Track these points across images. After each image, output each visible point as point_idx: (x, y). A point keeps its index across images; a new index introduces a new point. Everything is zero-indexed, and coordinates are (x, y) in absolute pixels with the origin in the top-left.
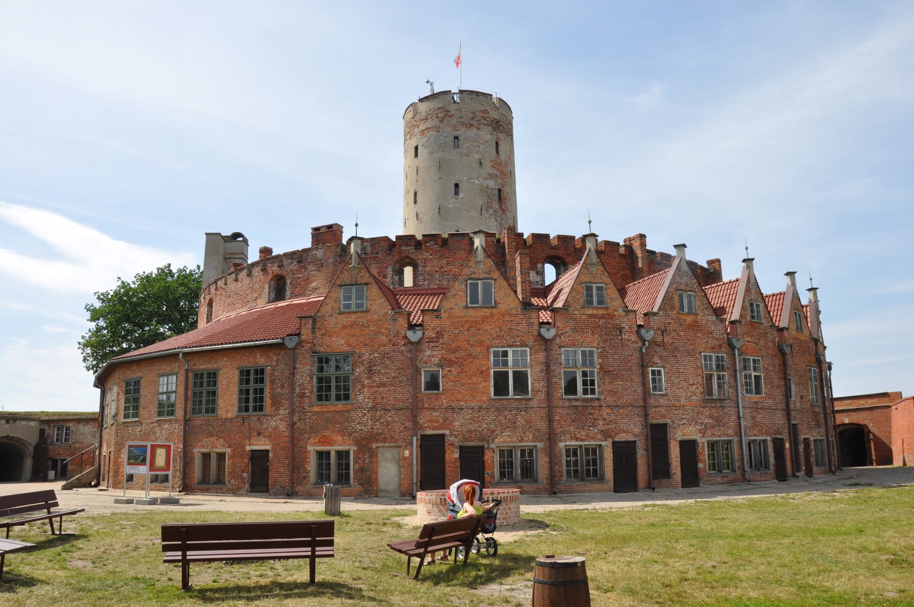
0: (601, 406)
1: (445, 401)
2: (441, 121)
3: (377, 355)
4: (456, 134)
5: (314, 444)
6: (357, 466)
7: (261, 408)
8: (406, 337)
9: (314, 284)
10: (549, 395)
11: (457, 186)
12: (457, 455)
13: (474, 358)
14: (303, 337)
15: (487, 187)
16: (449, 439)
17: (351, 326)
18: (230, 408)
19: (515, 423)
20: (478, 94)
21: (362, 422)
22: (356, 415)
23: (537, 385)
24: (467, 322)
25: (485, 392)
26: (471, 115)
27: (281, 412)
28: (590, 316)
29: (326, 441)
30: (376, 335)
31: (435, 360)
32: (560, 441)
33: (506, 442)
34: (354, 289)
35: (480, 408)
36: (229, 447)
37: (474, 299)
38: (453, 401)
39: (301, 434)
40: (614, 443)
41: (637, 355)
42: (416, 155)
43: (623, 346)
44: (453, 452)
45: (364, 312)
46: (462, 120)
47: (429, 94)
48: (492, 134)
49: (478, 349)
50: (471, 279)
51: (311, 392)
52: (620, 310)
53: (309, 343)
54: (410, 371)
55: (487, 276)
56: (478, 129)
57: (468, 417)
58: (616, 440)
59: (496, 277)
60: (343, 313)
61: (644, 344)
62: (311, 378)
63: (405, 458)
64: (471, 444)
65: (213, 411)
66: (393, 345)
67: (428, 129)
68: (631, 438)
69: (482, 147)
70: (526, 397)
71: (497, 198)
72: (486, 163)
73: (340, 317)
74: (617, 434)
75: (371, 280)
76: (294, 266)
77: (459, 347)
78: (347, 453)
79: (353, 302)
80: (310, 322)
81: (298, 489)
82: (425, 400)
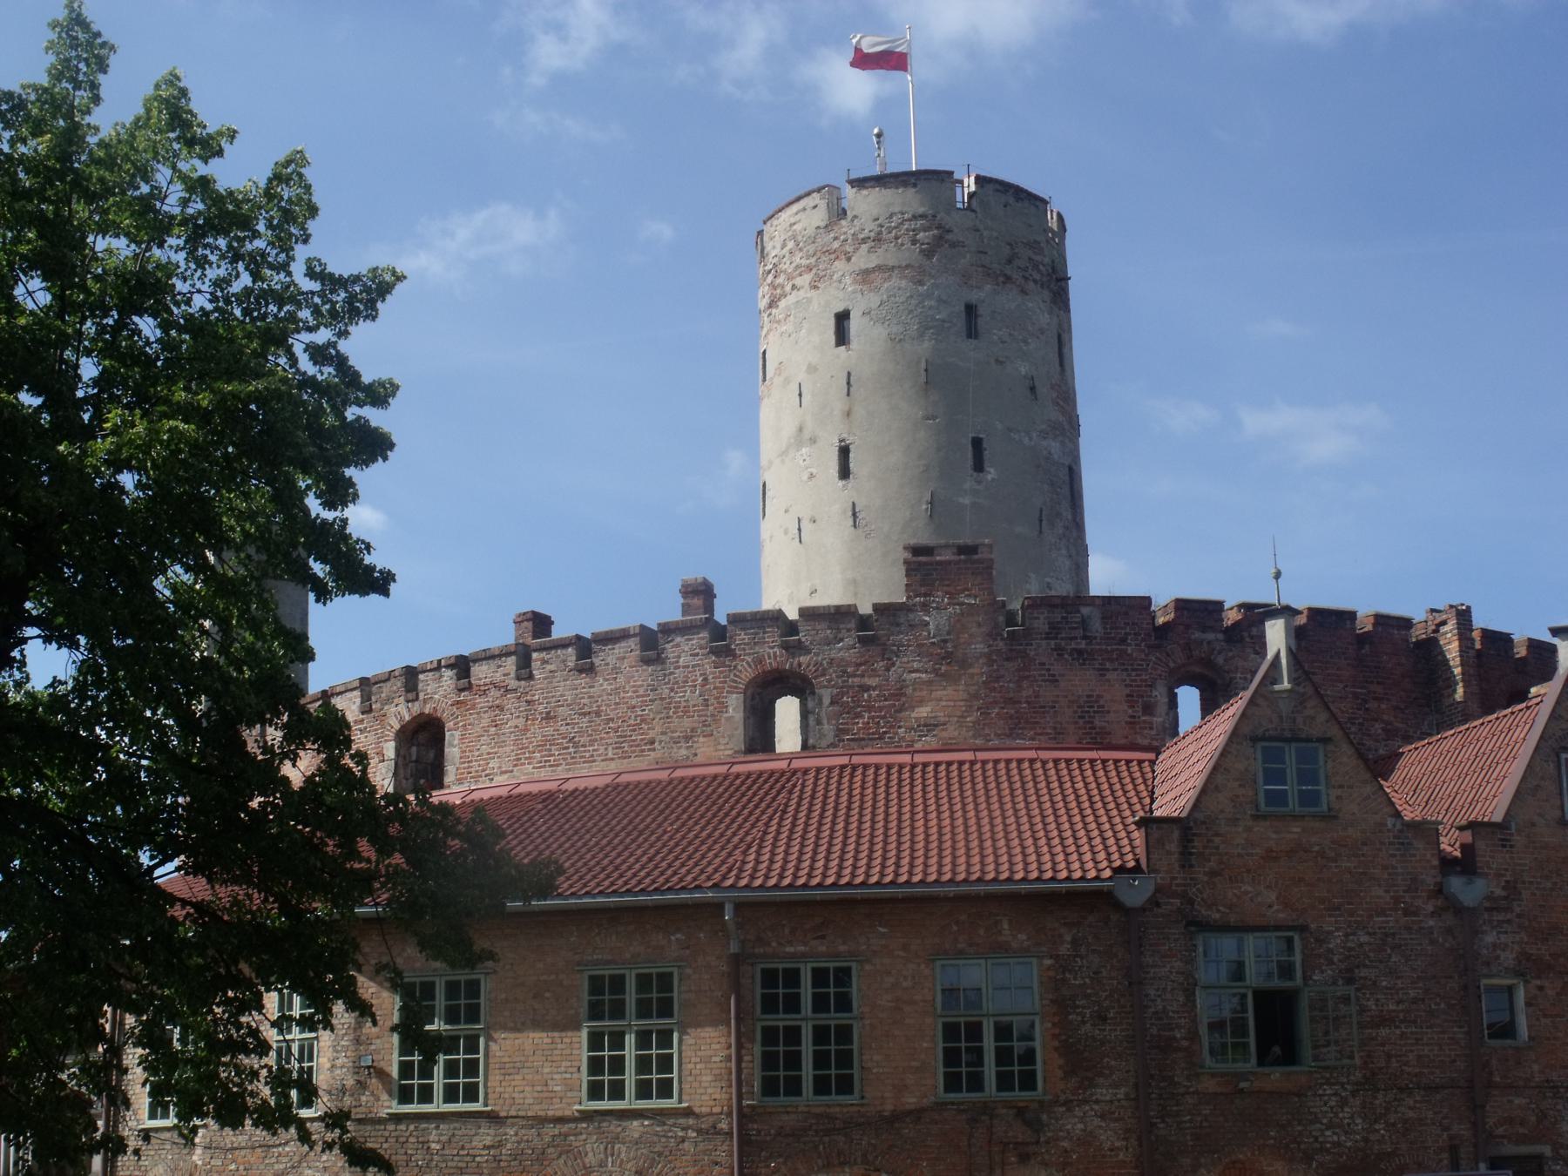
1: (1536, 1067)
3: (1364, 939)
4: (974, 296)
7: (1028, 1082)
8: (1439, 891)
9: (923, 712)
11: (977, 444)
26: (1007, 251)
27: (1103, 1093)
31: (1508, 958)
42: (842, 338)
45: (1323, 817)
48: (1050, 313)
56: (1024, 292)
60: (1265, 817)
65: (845, 1086)
66: (1406, 913)
71: (1066, 490)
75: (1334, 731)
76: (846, 648)
79: (1291, 787)
80: (1176, 835)
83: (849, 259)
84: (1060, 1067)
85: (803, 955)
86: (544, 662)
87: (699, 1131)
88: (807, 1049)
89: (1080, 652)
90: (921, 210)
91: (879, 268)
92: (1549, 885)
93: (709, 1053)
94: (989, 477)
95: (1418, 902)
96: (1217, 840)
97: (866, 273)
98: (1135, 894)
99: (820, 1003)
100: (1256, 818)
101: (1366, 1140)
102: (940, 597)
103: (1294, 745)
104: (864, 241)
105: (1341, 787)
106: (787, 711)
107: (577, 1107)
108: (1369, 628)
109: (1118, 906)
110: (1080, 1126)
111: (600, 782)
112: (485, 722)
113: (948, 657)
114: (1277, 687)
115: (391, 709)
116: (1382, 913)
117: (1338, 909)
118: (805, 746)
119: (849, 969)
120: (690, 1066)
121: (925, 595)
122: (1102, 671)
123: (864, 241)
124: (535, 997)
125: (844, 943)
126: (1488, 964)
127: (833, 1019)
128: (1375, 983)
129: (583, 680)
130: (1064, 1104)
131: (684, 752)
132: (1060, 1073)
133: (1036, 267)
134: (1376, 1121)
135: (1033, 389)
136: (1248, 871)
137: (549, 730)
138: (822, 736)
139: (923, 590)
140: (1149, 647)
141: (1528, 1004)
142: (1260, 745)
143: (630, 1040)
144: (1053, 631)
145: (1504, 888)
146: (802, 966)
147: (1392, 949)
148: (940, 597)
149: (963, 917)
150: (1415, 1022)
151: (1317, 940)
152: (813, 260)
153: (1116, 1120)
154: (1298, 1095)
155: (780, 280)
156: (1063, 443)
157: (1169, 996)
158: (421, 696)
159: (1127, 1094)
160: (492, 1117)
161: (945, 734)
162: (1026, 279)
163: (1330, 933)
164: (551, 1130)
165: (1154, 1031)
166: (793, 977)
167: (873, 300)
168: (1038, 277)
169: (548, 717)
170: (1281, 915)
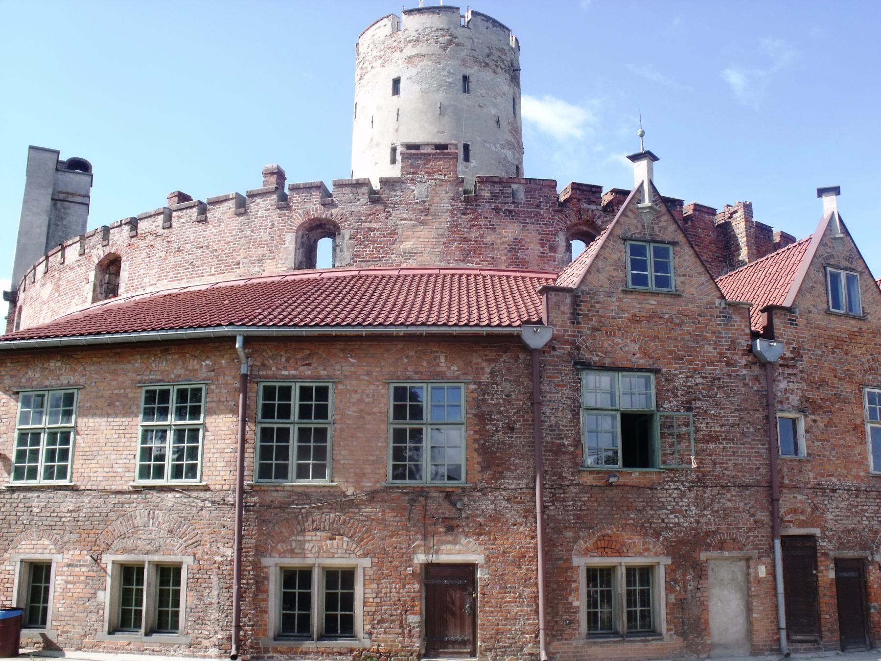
1: (811, 475)
4: (467, 72)
5: (586, 552)
6: (672, 598)
8: (750, 350)
12: (832, 575)
15: (505, 159)
16: (823, 544)
17: (649, 318)
18: (368, 469)
20: (495, 22)
21: (680, 509)
22: (669, 494)
24: (830, 337)
25: (862, 462)
26: (487, 51)
27: (509, 483)
29: (607, 546)
30: (696, 341)
31: (794, 399)
36: (365, 555)
38: (822, 475)
42: (396, 90)
44: (827, 569)
45: (671, 295)
46: (475, 54)
48: (510, 86)
53: (566, 342)
54: (759, 415)
56: (495, 72)
59: (860, 269)
63: (759, 581)
69: (499, 100)
72: (503, 123)
73: (628, 299)
75: (680, 238)
76: (362, 205)
79: (651, 273)
80: (568, 300)
82: (785, 470)
83: (401, 51)
84: (479, 463)
85: (294, 377)
86: (179, 217)
87: (213, 502)
88: (294, 443)
89: (510, 212)
90: (441, 26)
91: (417, 55)
92: (820, 352)
93: (224, 446)
94: (472, 165)
95: (736, 358)
96: (597, 306)
97: (410, 57)
98: (536, 339)
99: (305, 412)
100: (625, 292)
101: (698, 522)
102: (422, 175)
103: (652, 245)
104: (410, 42)
105: (684, 275)
106: (324, 246)
107: (132, 484)
108: (691, 212)
110: (492, 507)
111: (203, 288)
112: (144, 254)
113: (427, 211)
114: (640, 205)
115: (94, 252)
116: (712, 363)
117: (682, 359)
118: (334, 266)
119: (327, 388)
120: (210, 455)
121: (413, 173)
122: (525, 224)
123: (410, 42)
124: (109, 405)
125: (325, 369)
126: (781, 403)
127: (313, 423)
128: (706, 412)
129: (201, 227)
130: (481, 490)
131: (257, 269)
132: (478, 468)
133: (502, 61)
134: (705, 509)
135: (498, 122)
136: (619, 329)
137: (179, 259)
138: (343, 259)
140: (555, 211)
141: (807, 431)
142: (629, 243)
143: (170, 435)
144: (494, 196)
145: (792, 352)
146: (293, 385)
147: (718, 388)
148: (422, 175)
149: (412, 353)
150: (732, 440)
151: (666, 380)
152: (382, 53)
153: (519, 503)
154: (652, 489)
155: (366, 65)
156: (514, 153)
157: (560, 414)
158: (111, 243)
159: (527, 484)
160: (73, 489)
161: (421, 259)
163: (675, 375)
164: (113, 499)
165: (549, 439)
166: (286, 393)
167: (413, 71)
168: (501, 64)
169: (179, 250)
170: (642, 361)
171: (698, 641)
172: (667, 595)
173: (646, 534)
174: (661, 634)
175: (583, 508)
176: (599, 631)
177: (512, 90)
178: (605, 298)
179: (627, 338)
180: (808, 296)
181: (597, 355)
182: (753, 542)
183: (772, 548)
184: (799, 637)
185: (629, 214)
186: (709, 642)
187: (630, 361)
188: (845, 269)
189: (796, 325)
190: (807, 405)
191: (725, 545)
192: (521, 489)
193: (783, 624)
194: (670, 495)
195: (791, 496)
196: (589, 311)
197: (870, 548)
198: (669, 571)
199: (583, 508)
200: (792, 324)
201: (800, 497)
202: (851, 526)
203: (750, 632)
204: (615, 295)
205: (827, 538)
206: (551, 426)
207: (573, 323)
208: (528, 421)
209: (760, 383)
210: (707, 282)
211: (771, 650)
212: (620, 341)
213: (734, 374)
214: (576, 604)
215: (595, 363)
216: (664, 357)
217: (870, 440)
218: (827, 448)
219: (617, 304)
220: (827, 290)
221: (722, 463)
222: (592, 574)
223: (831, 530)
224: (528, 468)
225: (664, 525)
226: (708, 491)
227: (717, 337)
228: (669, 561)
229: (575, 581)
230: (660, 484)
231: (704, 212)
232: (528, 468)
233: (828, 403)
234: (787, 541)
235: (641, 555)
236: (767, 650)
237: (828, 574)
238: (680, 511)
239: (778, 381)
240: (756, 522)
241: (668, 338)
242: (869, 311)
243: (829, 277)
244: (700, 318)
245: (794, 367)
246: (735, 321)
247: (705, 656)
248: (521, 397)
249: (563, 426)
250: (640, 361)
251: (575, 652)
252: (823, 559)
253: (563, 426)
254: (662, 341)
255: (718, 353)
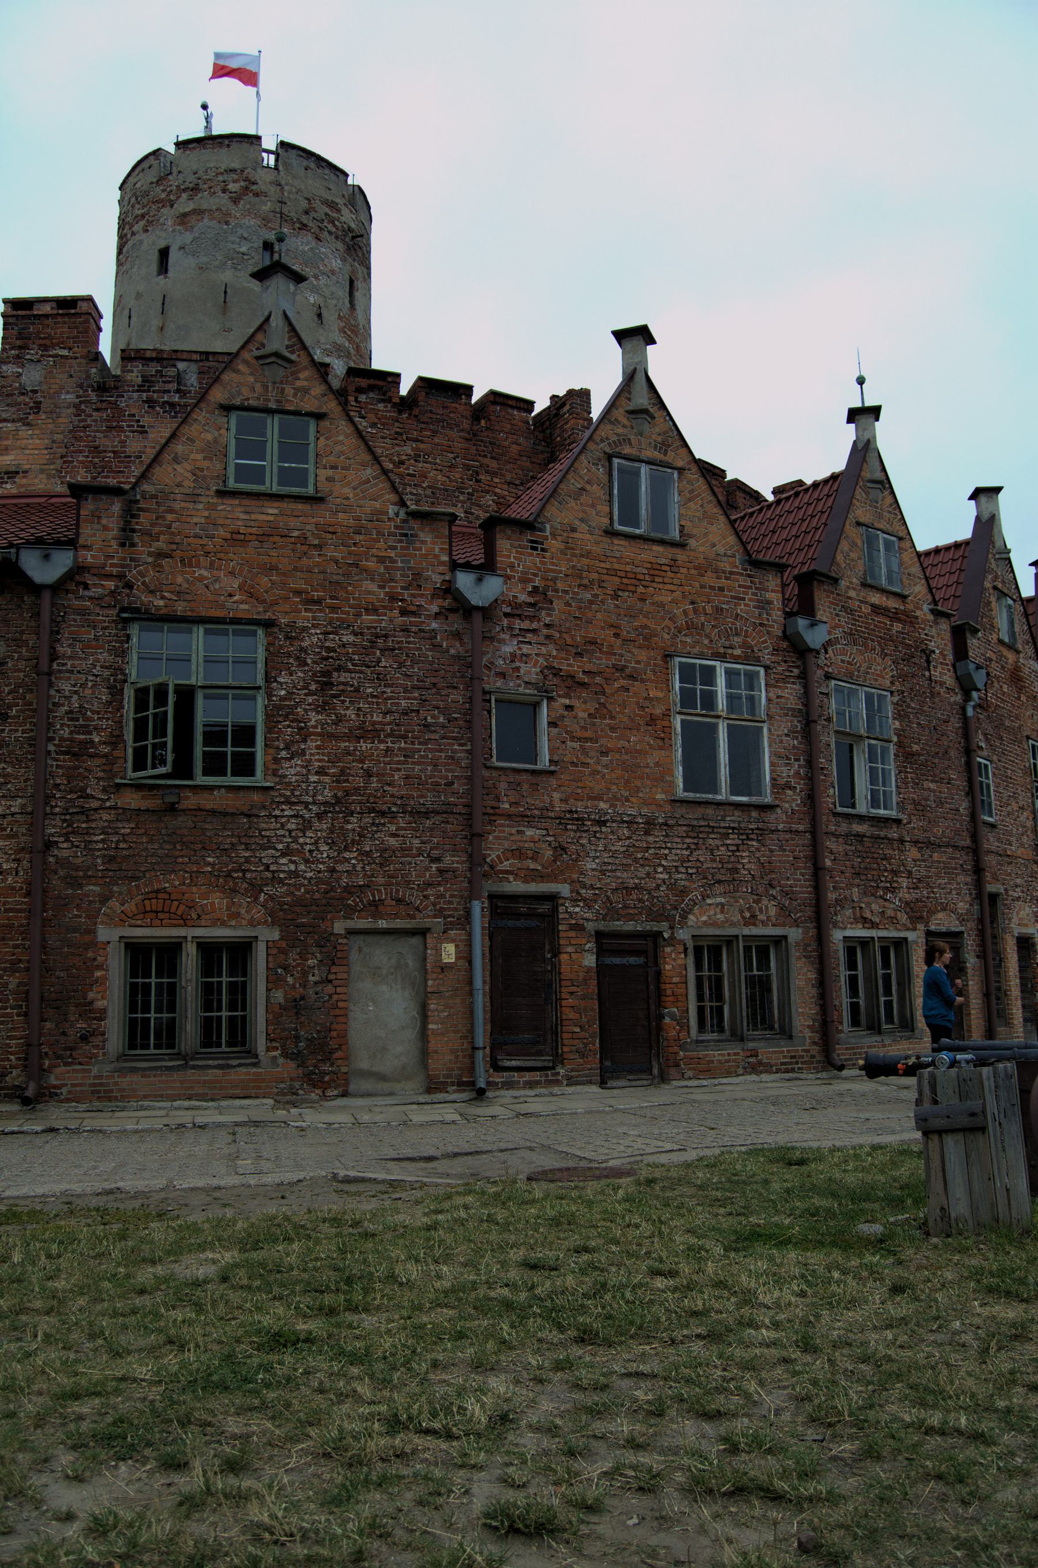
0: (902, 841)
1: (556, 796)
2: (235, 201)
5: (124, 919)
6: (279, 996)
8: (449, 590)
10: (811, 798)
12: (590, 960)
13: (631, 677)
14: (89, 557)
17: (263, 537)
19: (736, 871)
20: (319, 159)
23: (786, 773)
24: (611, 572)
25: (663, 776)
26: (304, 204)
28: (876, 609)
31: (530, 671)
32: (835, 925)
33: (715, 924)
34: (273, 426)
35: (650, 824)
37: (630, 516)
39: (74, 883)
40: (929, 934)
41: (956, 723)
43: (933, 695)
44: (581, 950)
47: (202, 135)
48: (344, 260)
49: (643, 655)
50: (619, 456)
51: (116, 740)
52: (926, 608)
53: (109, 576)
54: (457, 697)
55: (657, 455)
57: (618, 846)
58: (932, 928)
59: (680, 464)
61: (967, 697)
62: (116, 692)
63: (444, 968)
64: (630, 926)
66: (404, 612)
67: (199, 212)
68: (955, 926)
70: (754, 799)
73: (225, 506)
74: (932, 912)
77: (593, 642)
78: (240, 952)
79: (271, 463)
80: (117, 507)
81: (60, 1076)
82: (503, 786)
83: (172, 206)
89: (172, 405)
90: (233, 165)
91: (194, 212)
95: (418, 601)
96: (170, 517)
97: (185, 215)
100: (222, 494)
101: (333, 870)
104: (184, 190)
105: (332, 467)
109: (36, 589)
116: (375, 611)
121: (20, 348)
126: (503, 675)
128: (357, 690)
134: (346, 849)
135: (320, 316)
136: (207, 554)
139: (18, 343)
141: (552, 724)
144: (147, 382)
145: (530, 593)
151: (287, 637)
154: (248, 816)
159: (23, 806)
162: (321, 229)
163: (305, 629)
165: (66, 733)
168: (330, 227)
171: (327, 1067)
172: (268, 990)
173: (234, 891)
174: (256, 1056)
175: (122, 845)
176: (153, 1051)
177: (348, 268)
178: (183, 504)
179: (219, 569)
180: (572, 503)
181: (163, 597)
182: (434, 904)
183: (468, 913)
184: (514, 1063)
185: (241, 367)
186: (344, 1069)
187: (223, 607)
188: (648, 463)
189: (543, 550)
190: (555, 681)
191: (381, 908)
192: (13, 815)
193: (480, 1040)
194: (283, 826)
195: (514, 830)
196: (153, 525)
197: (670, 919)
198: (274, 951)
199: (122, 845)
200: (536, 549)
201: (529, 832)
202: (631, 883)
203: (424, 1054)
204: (202, 499)
205: (584, 900)
206: (71, 712)
207: (123, 545)
208: (31, 704)
209: (462, 644)
210: (374, 478)
211: (460, 1084)
212: (205, 573)
213: (414, 629)
214: (100, 1004)
215: (158, 608)
216: (286, 599)
217: (679, 742)
218: (592, 753)
219: (206, 514)
220: (611, 494)
221: (383, 775)
222: (138, 954)
223: (592, 887)
224: (25, 781)
225: (269, 875)
226: (354, 820)
227: (386, 568)
228: (276, 935)
229: (100, 967)
230: (264, 807)
231: (512, 407)
232: (25, 781)
233: (598, 679)
234: (502, 906)
235: (224, 924)
236: (453, 1084)
237: (580, 959)
238: (300, 852)
239: (500, 641)
240: (441, 871)
241: (296, 569)
242: (695, 531)
243: (615, 473)
244: (358, 538)
245: (532, 618)
246: (424, 542)
247: (336, 1092)
248: (22, 664)
249: (93, 712)
250: (245, 609)
251: (94, 1085)
252: (573, 934)
253: (93, 712)
254: (284, 574)
255: (386, 594)
